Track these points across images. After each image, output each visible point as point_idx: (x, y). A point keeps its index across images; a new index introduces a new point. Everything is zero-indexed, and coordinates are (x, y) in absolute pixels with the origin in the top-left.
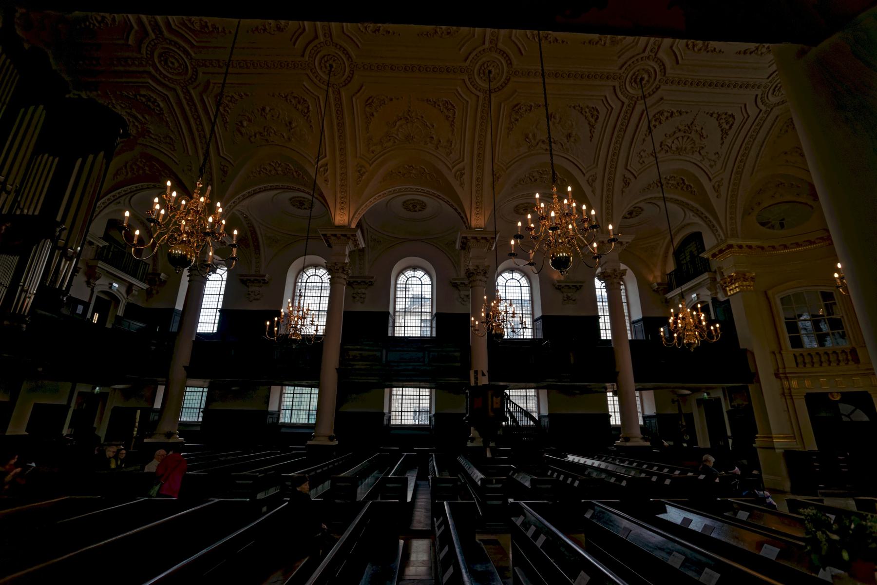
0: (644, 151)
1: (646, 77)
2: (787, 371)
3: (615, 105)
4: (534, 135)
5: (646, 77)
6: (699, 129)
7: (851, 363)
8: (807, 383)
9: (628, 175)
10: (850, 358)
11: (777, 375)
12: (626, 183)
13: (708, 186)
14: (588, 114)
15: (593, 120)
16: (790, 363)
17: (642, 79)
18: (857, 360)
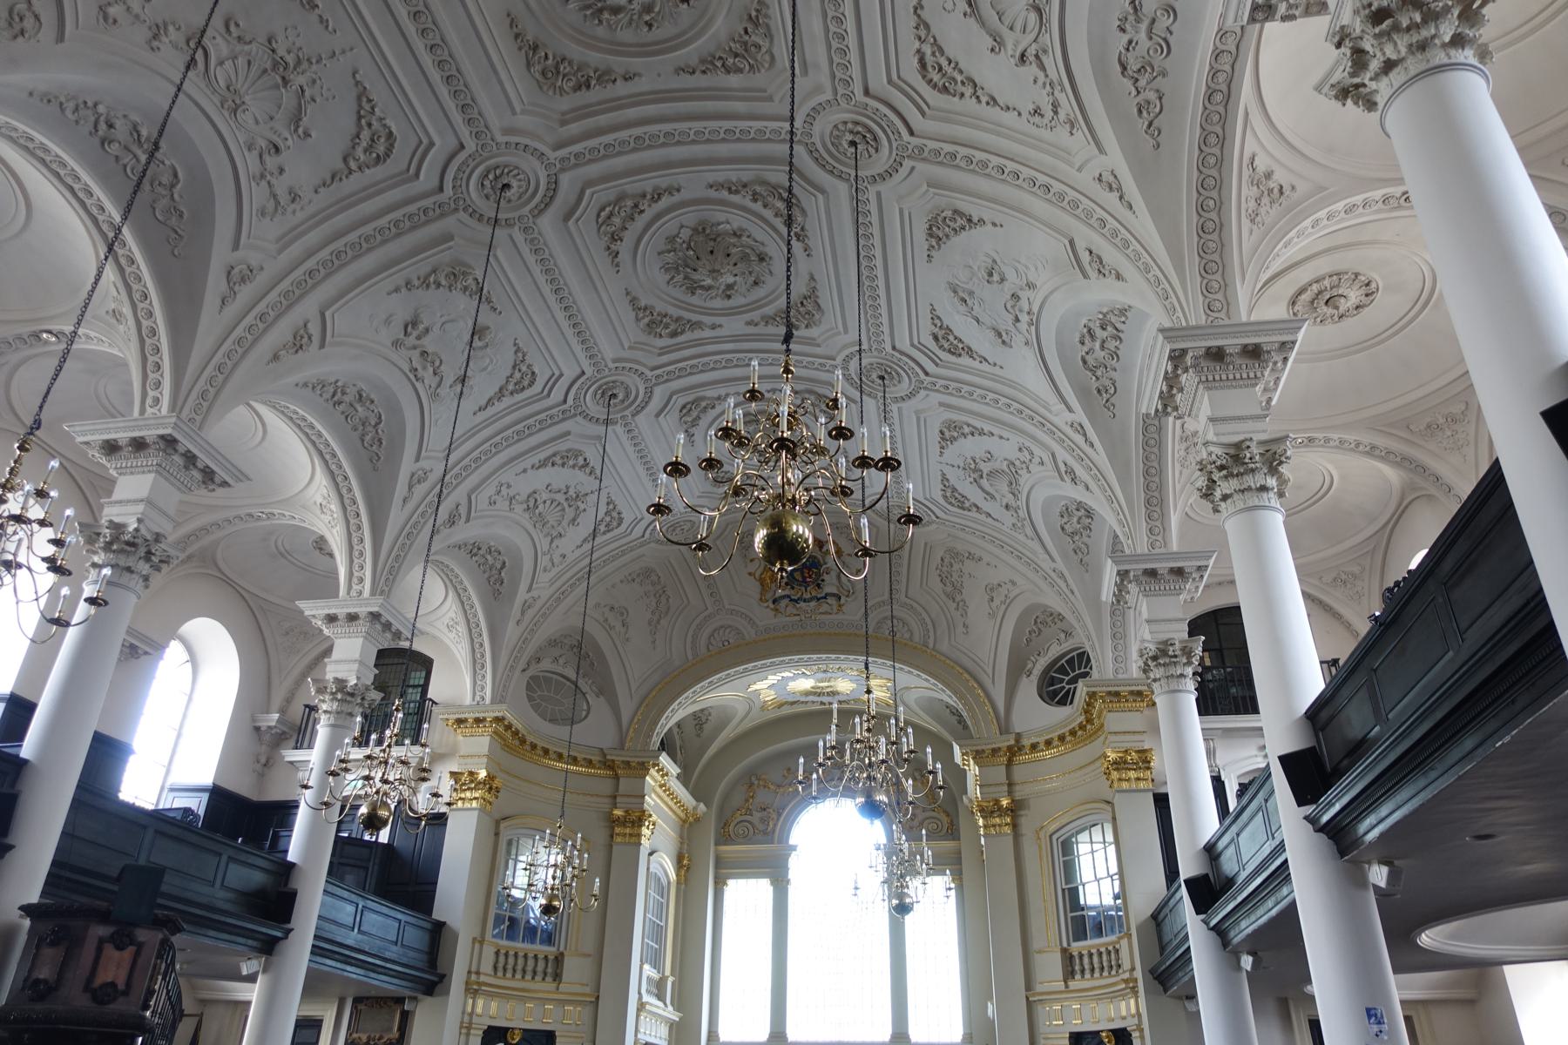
0: (509, 486)
1: (621, 396)
2: (483, 978)
3: (558, 394)
4: (427, 330)
5: (621, 396)
6: (582, 506)
7: (549, 979)
8: (494, 1005)
9: (463, 510)
10: (549, 970)
11: (467, 990)
12: (452, 521)
13: (522, 595)
14: (517, 375)
15: (511, 387)
16: (487, 967)
17: (614, 396)
18: (557, 977)
